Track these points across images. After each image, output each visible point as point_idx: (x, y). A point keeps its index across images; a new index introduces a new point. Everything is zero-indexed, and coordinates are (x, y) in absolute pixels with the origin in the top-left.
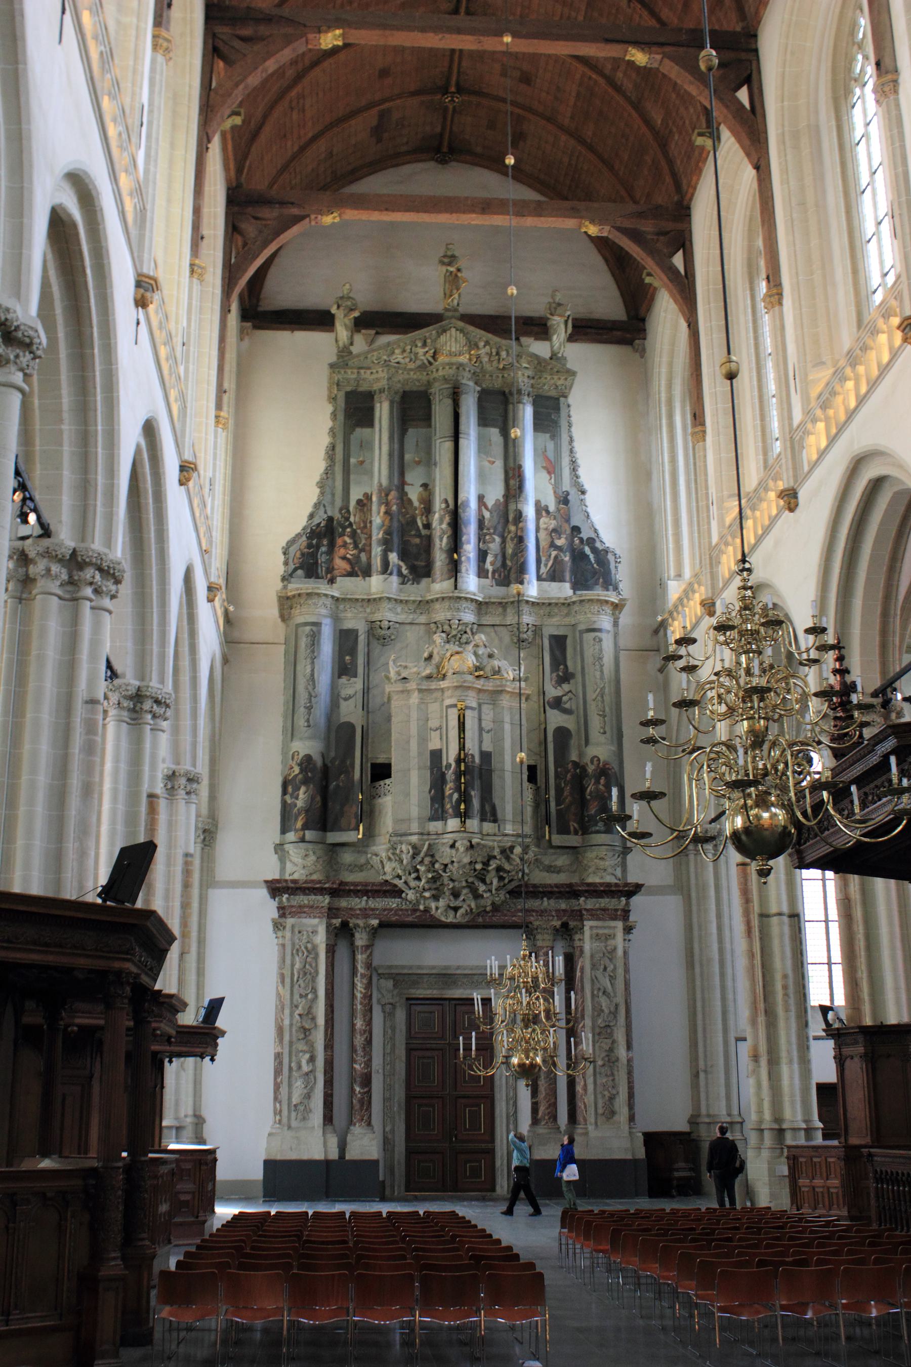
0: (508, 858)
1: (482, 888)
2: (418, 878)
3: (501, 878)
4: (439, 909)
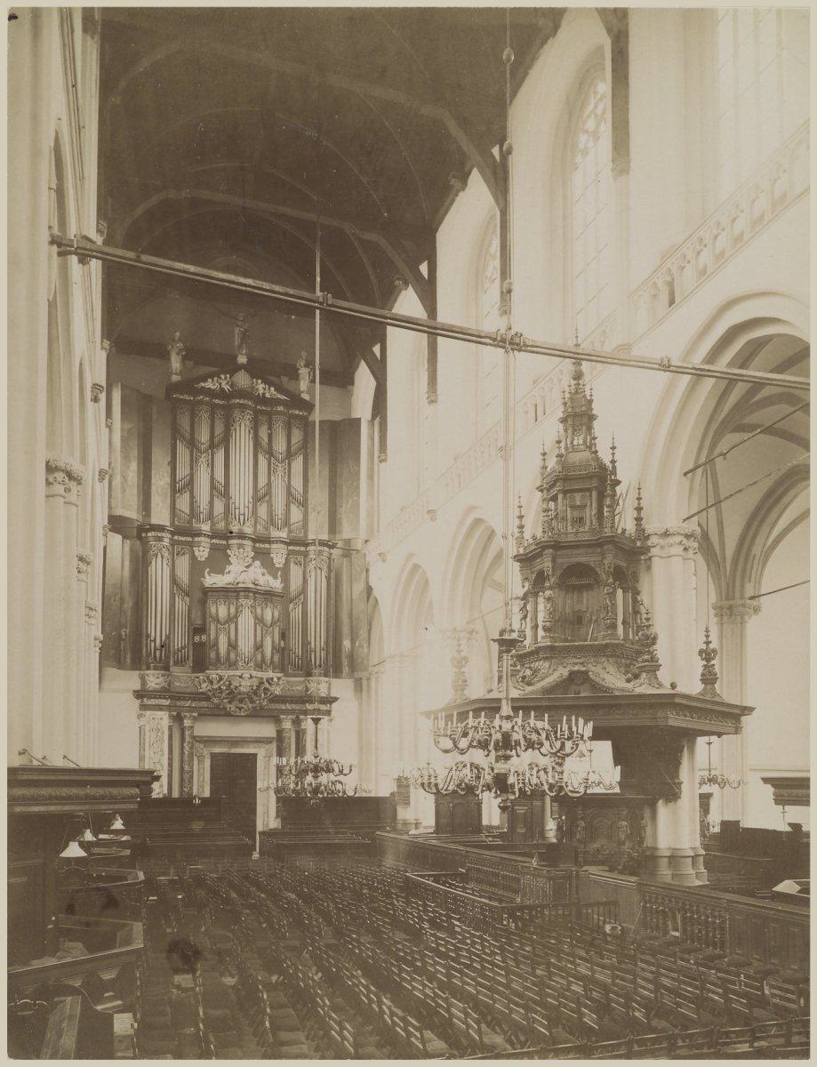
0: (270, 684)
1: (255, 698)
2: (221, 693)
3: (266, 694)
4: (232, 707)
